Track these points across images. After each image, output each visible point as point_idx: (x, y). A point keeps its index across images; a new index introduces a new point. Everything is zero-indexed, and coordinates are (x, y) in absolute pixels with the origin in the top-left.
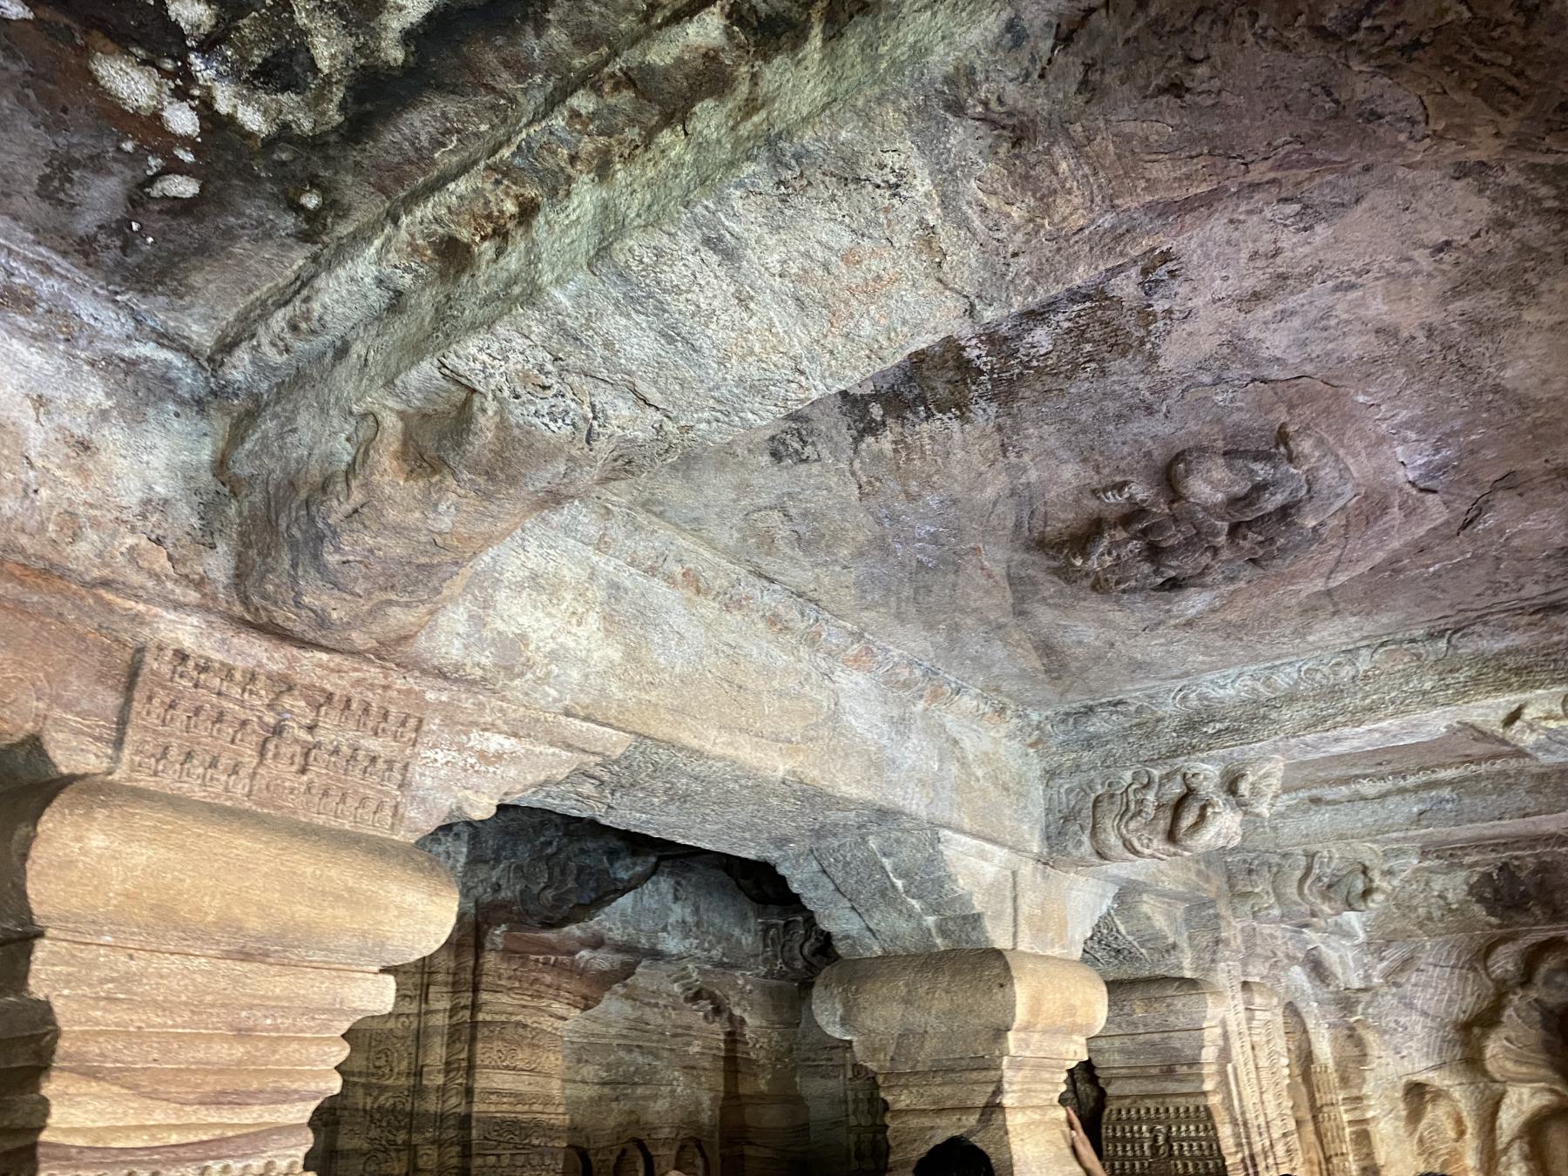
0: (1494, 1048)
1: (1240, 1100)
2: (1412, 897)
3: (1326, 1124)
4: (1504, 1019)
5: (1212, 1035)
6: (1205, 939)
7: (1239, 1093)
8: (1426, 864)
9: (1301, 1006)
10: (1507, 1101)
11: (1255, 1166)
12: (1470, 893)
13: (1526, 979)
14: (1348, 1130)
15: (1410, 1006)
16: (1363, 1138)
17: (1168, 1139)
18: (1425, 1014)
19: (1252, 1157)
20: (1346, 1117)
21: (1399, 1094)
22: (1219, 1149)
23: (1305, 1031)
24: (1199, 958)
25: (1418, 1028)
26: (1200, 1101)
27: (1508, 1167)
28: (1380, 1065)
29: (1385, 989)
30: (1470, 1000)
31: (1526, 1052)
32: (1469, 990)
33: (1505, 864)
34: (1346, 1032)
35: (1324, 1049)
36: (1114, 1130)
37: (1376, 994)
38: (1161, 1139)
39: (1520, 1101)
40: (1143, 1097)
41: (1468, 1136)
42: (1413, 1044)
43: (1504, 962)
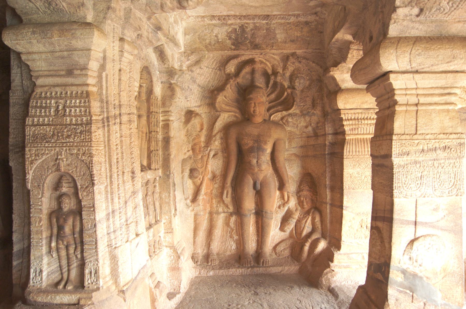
0: (220, 98)
1: (107, 90)
2: (205, 35)
3: (153, 119)
4: (226, 89)
5: (96, 54)
6: (102, 6)
7: (107, 87)
8: (214, 22)
9: (152, 70)
10: (220, 118)
11: (108, 122)
12: (227, 36)
13: (237, 73)
14: (161, 123)
15: (194, 82)
16: (167, 126)
17: (64, 107)
18: (199, 86)
19: (108, 118)
20: (161, 119)
21: (183, 113)
22: (90, 112)
23: (152, 81)
24: (97, 16)
25: (196, 91)
26: (85, 88)
27: (214, 141)
28: (179, 101)
29: (187, 72)
30: (216, 82)
31: (230, 102)
32: (216, 78)
33: (243, 25)
34: (168, 85)
35: (158, 90)
36: (37, 103)
37: (183, 73)
38: (60, 108)
39: (224, 119)
40: (54, 86)
41: (204, 131)
42: (193, 96)
43: (231, 68)
